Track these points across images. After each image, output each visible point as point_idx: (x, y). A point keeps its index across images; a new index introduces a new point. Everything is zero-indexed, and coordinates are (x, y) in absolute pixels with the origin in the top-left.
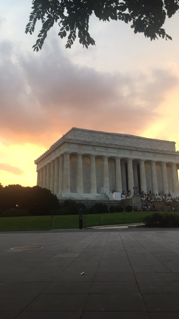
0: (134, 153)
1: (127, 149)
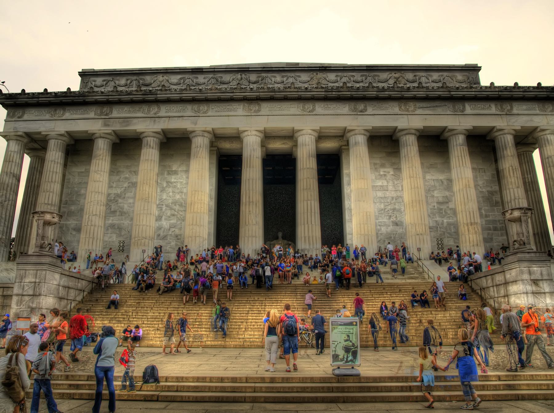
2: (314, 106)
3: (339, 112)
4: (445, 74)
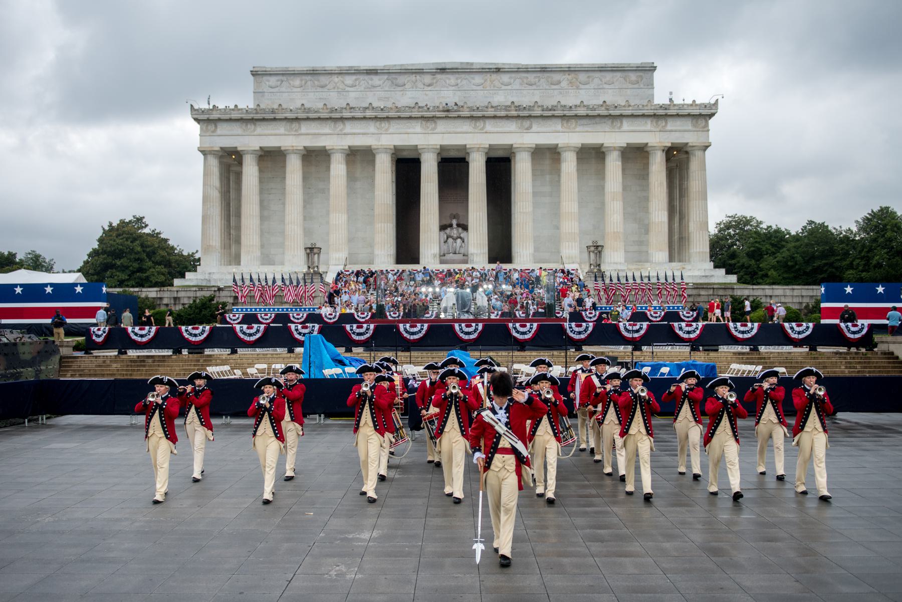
0: (442, 126)
1: (410, 118)
2: (485, 124)
3: (507, 129)
4: (619, 74)
